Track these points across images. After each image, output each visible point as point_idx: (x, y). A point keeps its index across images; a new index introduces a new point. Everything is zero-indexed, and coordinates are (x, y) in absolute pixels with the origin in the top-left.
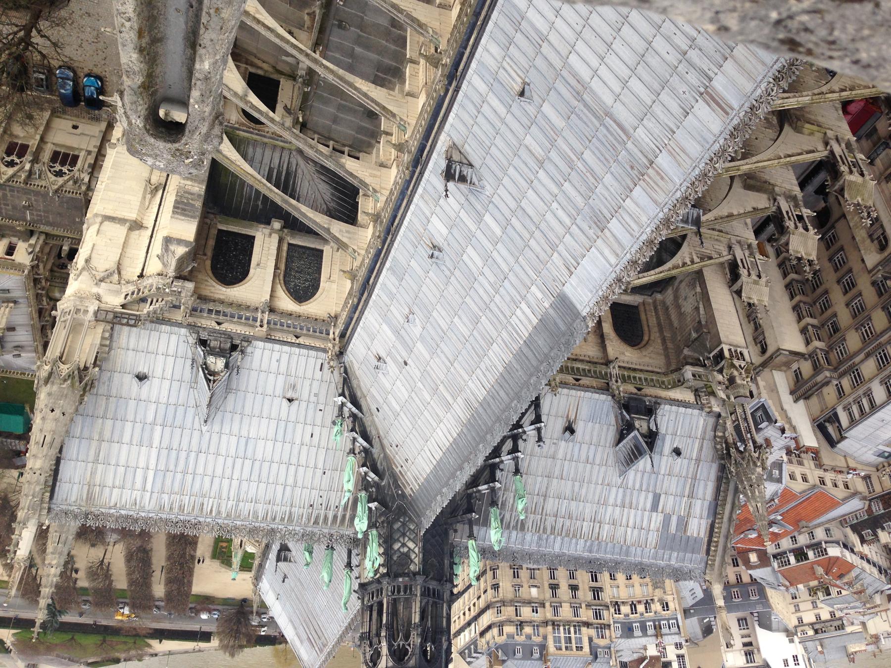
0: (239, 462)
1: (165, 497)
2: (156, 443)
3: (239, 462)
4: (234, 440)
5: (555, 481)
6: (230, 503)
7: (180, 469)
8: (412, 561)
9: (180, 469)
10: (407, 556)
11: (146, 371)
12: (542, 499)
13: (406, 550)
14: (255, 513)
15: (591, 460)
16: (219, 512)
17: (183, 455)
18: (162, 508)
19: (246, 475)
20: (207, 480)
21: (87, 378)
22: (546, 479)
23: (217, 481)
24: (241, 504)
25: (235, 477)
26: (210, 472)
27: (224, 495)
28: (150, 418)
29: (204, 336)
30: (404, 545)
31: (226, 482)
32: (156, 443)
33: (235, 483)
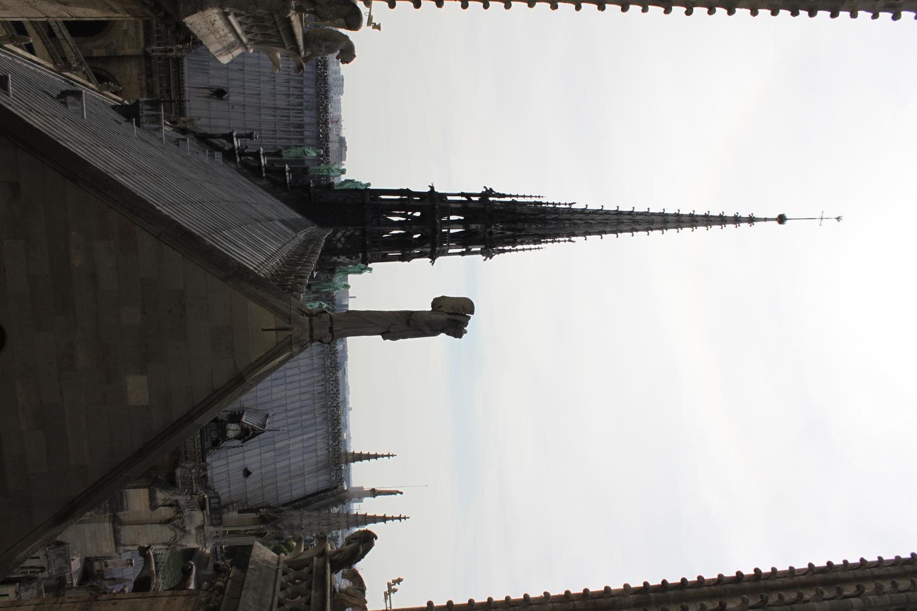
0: (288, 380)
1: (318, 420)
2: (286, 442)
3: (288, 380)
4: (275, 390)
5: (263, 101)
6: (315, 375)
7: (299, 418)
8: (352, 234)
9: (299, 418)
10: (348, 239)
11: (241, 472)
12: (278, 112)
13: (343, 239)
14: (319, 354)
15: (240, 67)
16: (322, 380)
17: (290, 420)
18: (326, 419)
19: (296, 371)
20: (303, 397)
21: (271, 514)
22: (263, 111)
23: (303, 390)
24: (315, 366)
25: (297, 378)
26: (298, 397)
27: (311, 381)
28: (272, 453)
29: (208, 444)
30: (339, 240)
31: (303, 384)
32: (286, 442)
33: (302, 377)
